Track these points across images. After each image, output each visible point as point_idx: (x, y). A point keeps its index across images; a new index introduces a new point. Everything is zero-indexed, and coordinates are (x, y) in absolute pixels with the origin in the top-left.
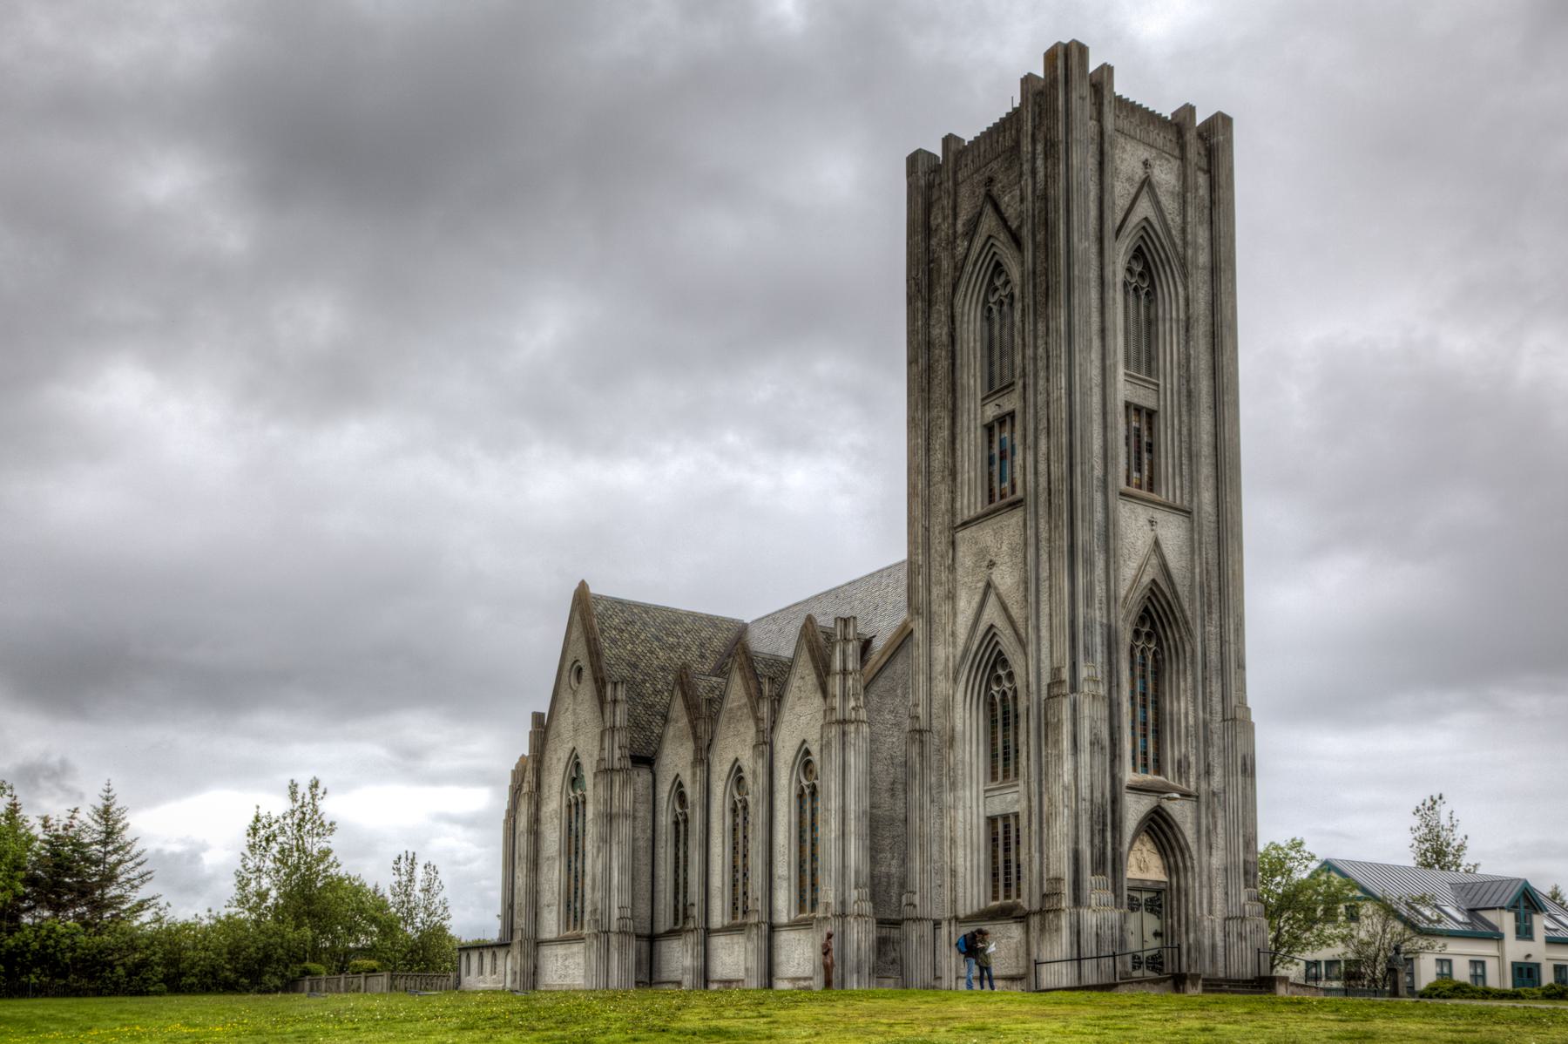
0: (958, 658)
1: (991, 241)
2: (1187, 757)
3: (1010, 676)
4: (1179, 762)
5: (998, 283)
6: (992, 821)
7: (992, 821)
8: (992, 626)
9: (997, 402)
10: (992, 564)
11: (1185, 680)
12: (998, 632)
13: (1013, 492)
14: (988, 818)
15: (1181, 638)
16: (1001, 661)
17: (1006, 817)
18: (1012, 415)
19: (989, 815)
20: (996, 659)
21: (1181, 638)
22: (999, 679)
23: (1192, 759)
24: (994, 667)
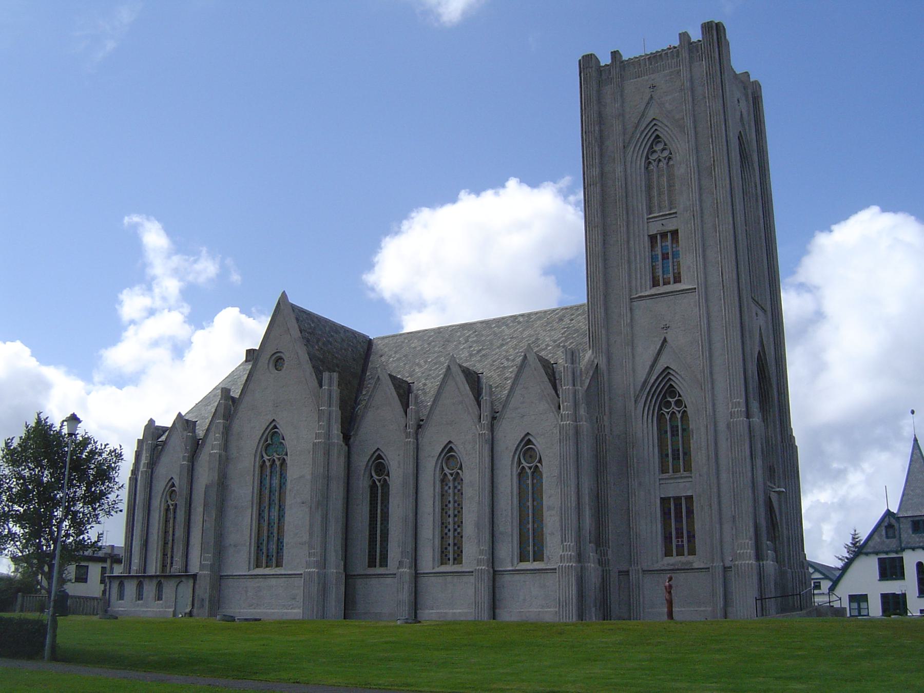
0: (639, 388)
1: (654, 122)
2: (773, 466)
3: (679, 403)
4: (770, 467)
5: (659, 147)
6: (664, 501)
7: (664, 501)
8: (668, 367)
9: (663, 222)
10: (666, 328)
11: (770, 416)
12: (671, 372)
13: (677, 279)
14: (661, 498)
15: (767, 388)
16: (672, 391)
17: (677, 499)
18: (675, 233)
19: (663, 496)
20: (666, 390)
21: (767, 388)
22: (668, 404)
23: (775, 466)
24: (664, 397)
